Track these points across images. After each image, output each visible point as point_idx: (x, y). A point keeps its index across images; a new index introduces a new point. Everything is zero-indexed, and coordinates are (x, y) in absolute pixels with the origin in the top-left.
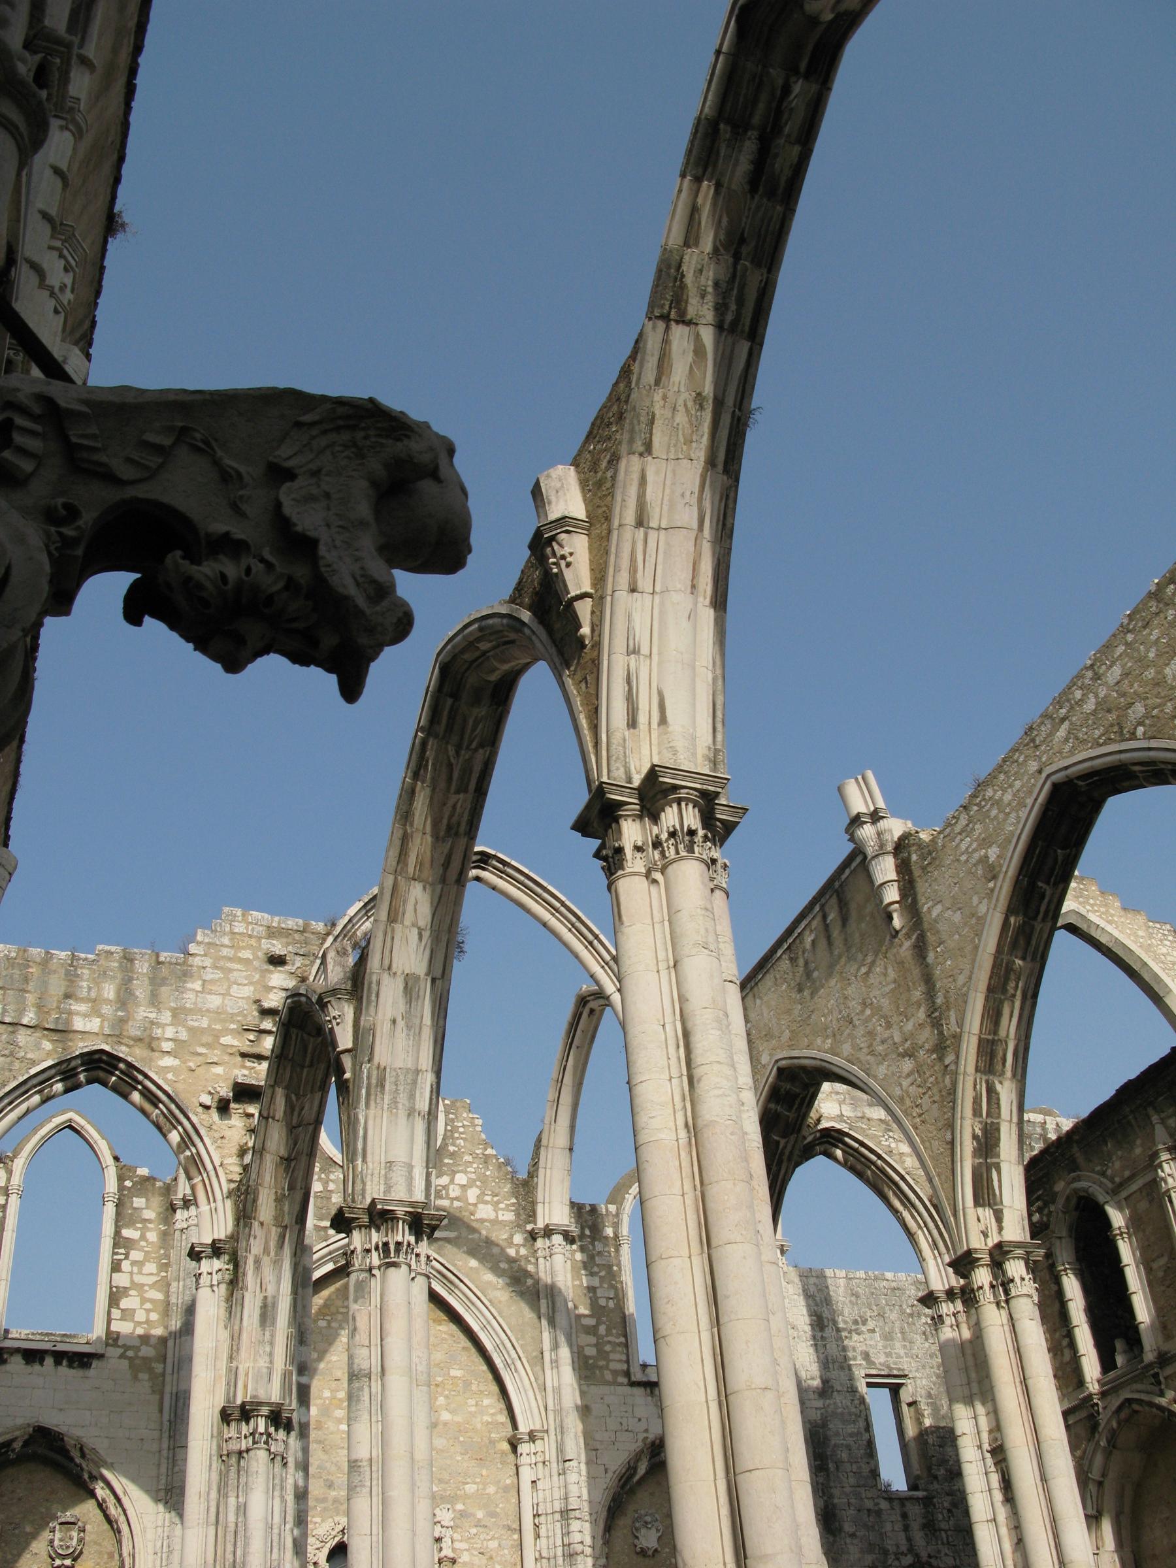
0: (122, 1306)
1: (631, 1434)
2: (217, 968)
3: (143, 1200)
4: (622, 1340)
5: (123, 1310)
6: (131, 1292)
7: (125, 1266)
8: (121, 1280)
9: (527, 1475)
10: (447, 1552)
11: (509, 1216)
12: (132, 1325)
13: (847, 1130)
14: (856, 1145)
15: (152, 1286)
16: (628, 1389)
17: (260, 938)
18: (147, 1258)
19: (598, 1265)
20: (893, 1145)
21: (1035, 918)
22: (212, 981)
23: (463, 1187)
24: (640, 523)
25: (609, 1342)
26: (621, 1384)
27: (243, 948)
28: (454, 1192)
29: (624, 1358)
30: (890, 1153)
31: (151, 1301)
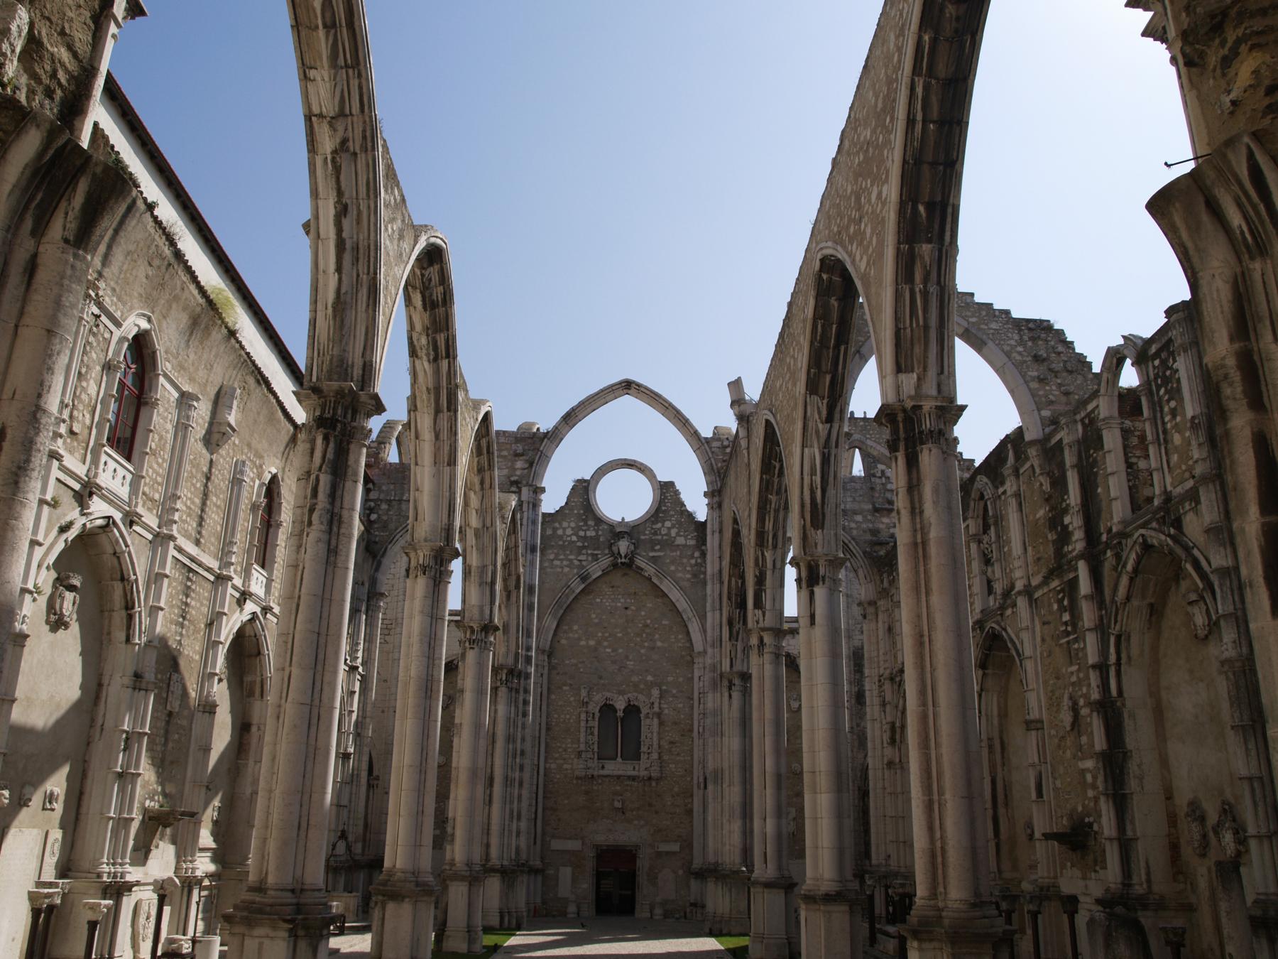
9: (696, 674)
10: (656, 709)
11: (692, 542)
23: (669, 529)
24: (417, 437)
28: (664, 531)
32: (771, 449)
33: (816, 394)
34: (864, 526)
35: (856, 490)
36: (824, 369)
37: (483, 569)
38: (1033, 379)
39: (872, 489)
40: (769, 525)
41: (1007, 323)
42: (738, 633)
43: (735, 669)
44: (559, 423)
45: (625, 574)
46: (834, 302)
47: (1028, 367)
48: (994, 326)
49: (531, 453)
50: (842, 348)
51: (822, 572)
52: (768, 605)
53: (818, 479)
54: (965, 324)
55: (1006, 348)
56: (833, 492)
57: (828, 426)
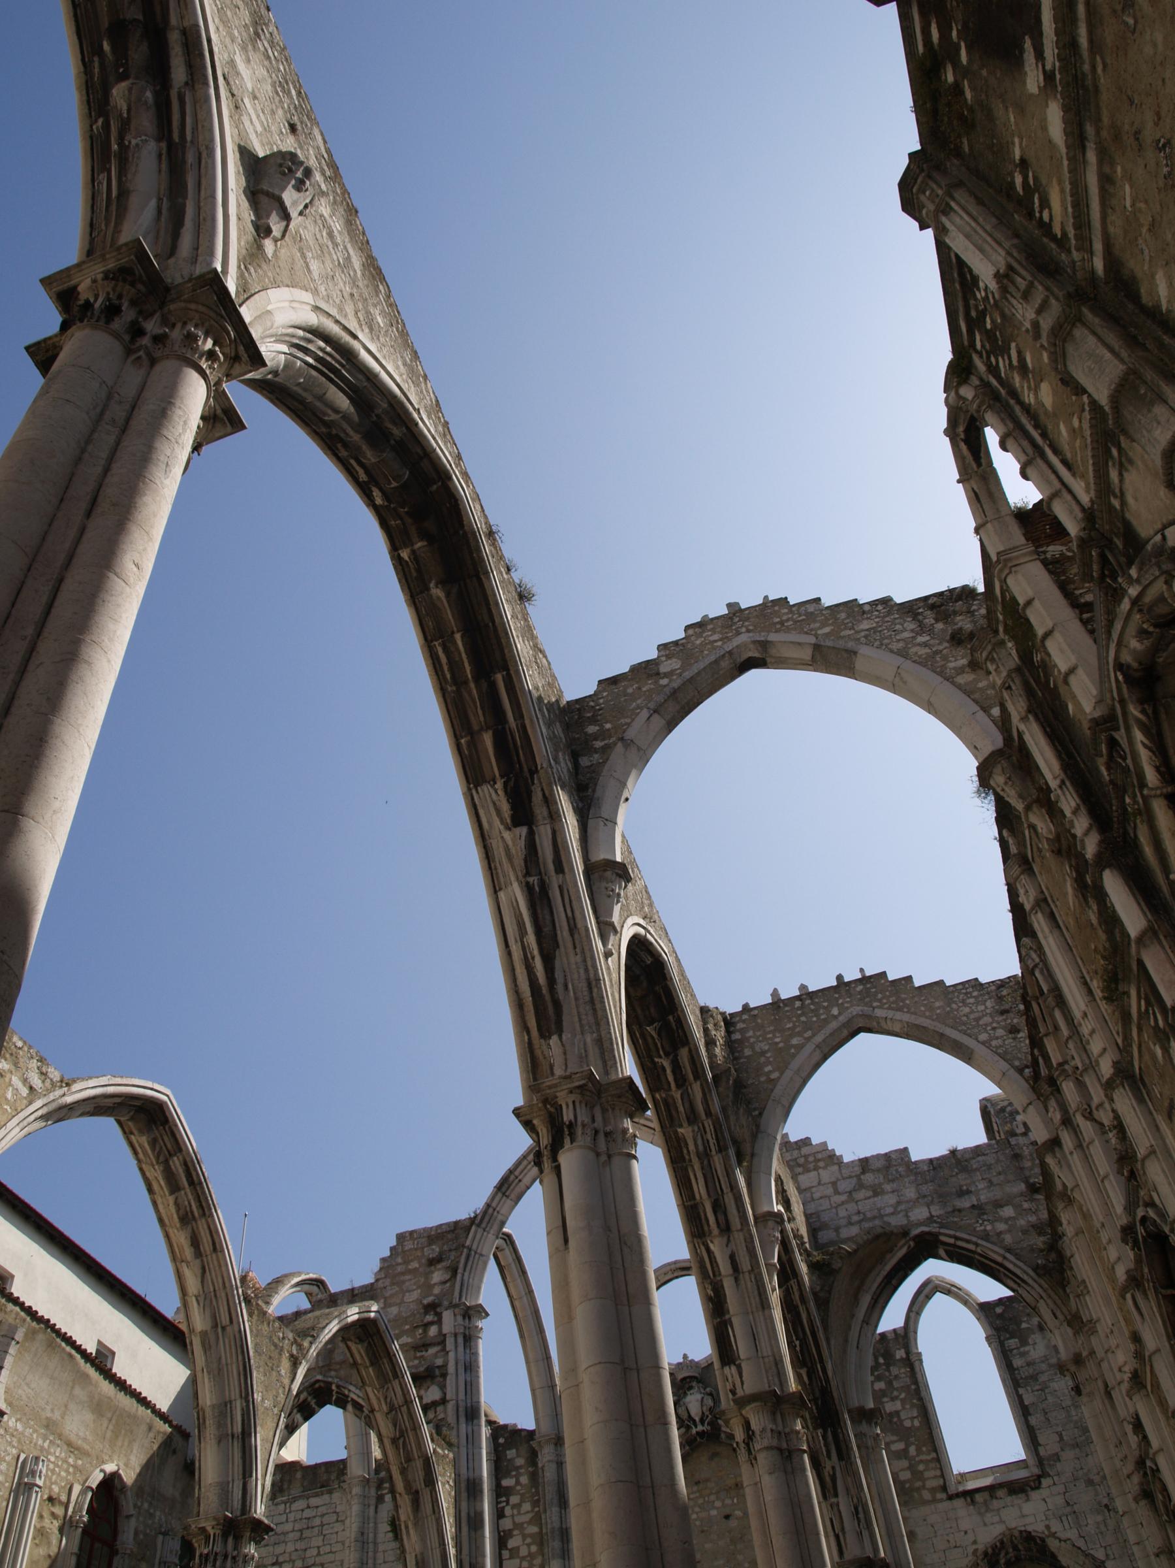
0: (509, 1547)
1: (960, 1550)
2: (393, 1284)
3: (514, 1451)
4: (934, 1455)
5: (510, 1550)
6: (515, 1532)
7: (508, 1511)
8: (506, 1524)
12: (518, 1561)
13: (937, 1230)
14: (952, 1241)
15: (530, 1522)
16: (947, 1505)
17: (423, 1248)
18: (522, 1501)
19: (897, 1389)
20: (989, 1228)
21: (670, 1089)
22: (392, 1296)
25: (921, 1461)
26: (941, 1500)
27: (412, 1261)
29: (938, 1473)
30: (986, 1236)
31: (531, 1535)
32: (643, 1035)
33: (485, 782)
34: (1022, 1222)
35: (989, 1167)
36: (476, 727)
37: (224, 1408)
38: (960, 671)
39: (1017, 1157)
40: (700, 1188)
41: (889, 613)
42: (833, 1478)
43: (848, 1556)
44: (493, 1197)
45: (715, 1455)
46: (437, 592)
47: (945, 659)
48: (865, 625)
49: (453, 1255)
50: (499, 678)
51: (568, 1115)
52: (742, 1347)
53: (531, 938)
54: (813, 640)
55: (895, 646)
56: (575, 959)
57: (524, 830)
